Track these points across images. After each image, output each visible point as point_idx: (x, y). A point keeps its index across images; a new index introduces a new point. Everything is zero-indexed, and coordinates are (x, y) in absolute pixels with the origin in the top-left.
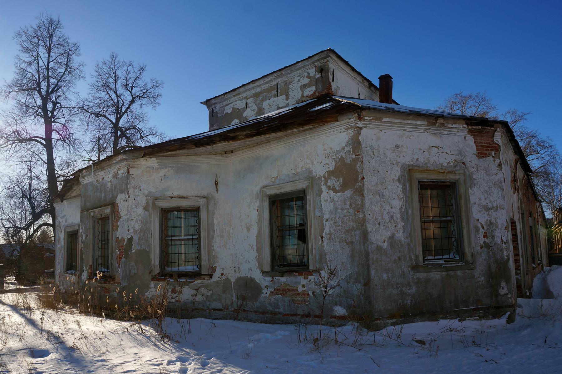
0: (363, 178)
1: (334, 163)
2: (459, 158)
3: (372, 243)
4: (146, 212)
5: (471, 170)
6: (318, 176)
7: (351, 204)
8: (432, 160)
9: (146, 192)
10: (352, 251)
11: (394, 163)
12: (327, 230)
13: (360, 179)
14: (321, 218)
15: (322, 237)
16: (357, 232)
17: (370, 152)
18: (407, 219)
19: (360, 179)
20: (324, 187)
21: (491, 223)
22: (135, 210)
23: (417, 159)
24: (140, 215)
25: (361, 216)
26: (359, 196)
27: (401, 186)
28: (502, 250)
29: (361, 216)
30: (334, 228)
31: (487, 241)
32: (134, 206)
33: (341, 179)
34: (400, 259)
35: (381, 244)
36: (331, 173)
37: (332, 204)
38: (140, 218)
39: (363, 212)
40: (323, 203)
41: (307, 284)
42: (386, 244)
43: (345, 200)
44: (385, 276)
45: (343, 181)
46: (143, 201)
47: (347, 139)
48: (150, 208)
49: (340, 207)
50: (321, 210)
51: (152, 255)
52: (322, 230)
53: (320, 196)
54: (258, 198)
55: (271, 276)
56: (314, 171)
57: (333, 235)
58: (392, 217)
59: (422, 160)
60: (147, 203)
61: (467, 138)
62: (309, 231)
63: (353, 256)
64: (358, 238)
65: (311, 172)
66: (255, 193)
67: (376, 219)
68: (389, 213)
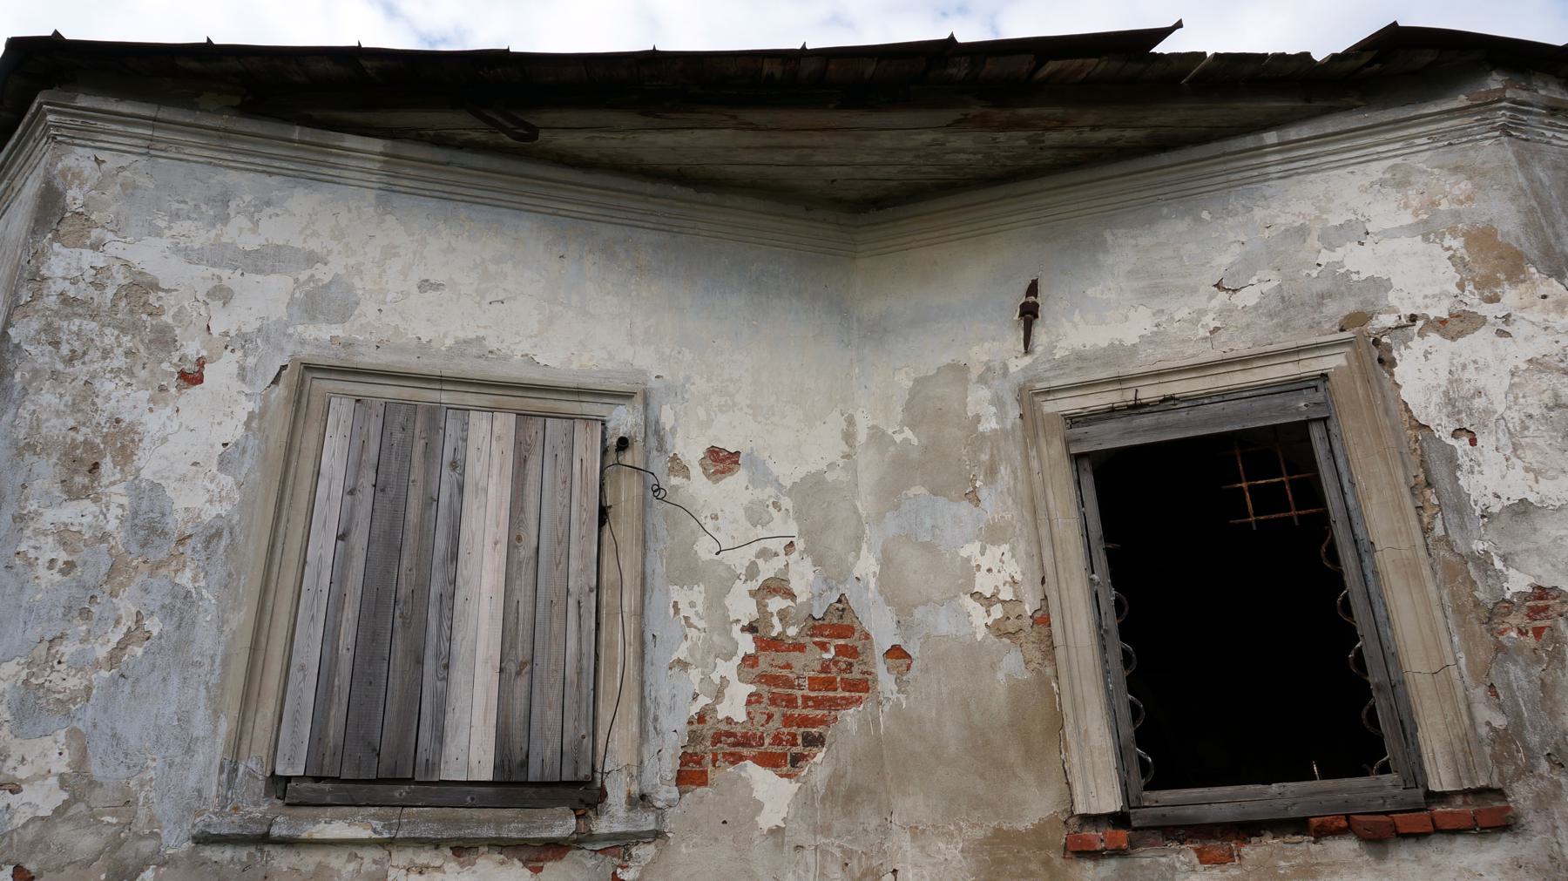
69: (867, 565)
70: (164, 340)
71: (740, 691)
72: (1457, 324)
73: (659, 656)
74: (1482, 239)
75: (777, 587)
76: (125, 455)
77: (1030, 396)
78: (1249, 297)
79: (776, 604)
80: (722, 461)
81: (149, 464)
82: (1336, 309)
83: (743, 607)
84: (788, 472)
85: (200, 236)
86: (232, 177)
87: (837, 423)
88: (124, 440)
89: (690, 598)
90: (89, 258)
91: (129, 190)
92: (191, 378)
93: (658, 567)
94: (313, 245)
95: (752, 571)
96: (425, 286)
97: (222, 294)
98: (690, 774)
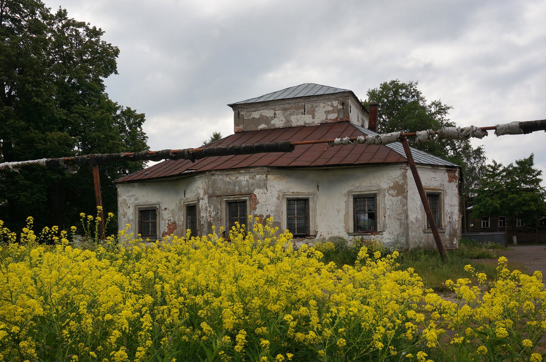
0: (407, 192)
1: (393, 183)
4: (278, 201)
6: (384, 188)
7: (401, 203)
9: (278, 190)
10: (400, 223)
12: (388, 213)
13: (406, 192)
14: (385, 208)
15: (385, 217)
16: (404, 215)
17: (410, 180)
19: (406, 192)
20: (387, 194)
21: (452, 213)
24: (274, 202)
25: (405, 208)
26: (405, 199)
29: (405, 208)
30: (392, 213)
32: (271, 197)
33: (396, 191)
36: (391, 188)
37: (391, 202)
38: (274, 204)
39: (407, 206)
40: (386, 201)
41: (376, 238)
43: (398, 201)
45: (397, 192)
46: (276, 194)
47: (400, 173)
48: (281, 198)
49: (395, 203)
50: (385, 204)
52: (385, 213)
53: (384, 198)
54: (346, 196)
55: (353, 236)
56: (381, 186)
57: (391, 216)
60: (279, 196)
62: (378, 213)
63: (401, 225)
64: (403, 217)
65: (379, 186)
66: (344, 193)
69: (177, 217)
70: (127, 205)
71: (167, 229)
72: (203, 199)
73: (161, 227)
74: (205, 190)
75: (170, 220)
76: (126, 215)
77: (184, 202)
78: (195, 194)
79: (170, 222)
80: (166, 209)
81: (128, 215)
82: (198, 196)
83: (167, 222)
84: (171, 209)
85: (127, 195)
86: (129, 189)
87: (175, 203)
88: (126, 213)
89: (163, 222)
90: (122, 198)
91: (123, 191)
92: (129, 208)
93: (161, 219)
94: (135, 194)
95: (168, 219)
96: (143, 196)
97: (130, 200)
98: (163, 236)
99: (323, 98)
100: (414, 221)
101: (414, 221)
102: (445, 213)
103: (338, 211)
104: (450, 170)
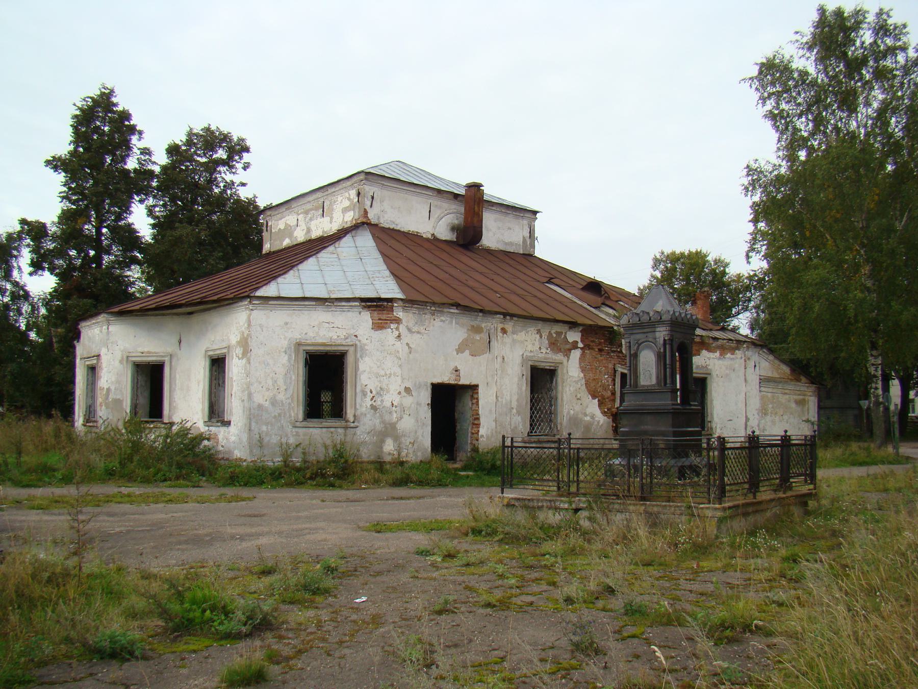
2: (352, 331)
3: (254, 402)
5: (364, 341)
8: (321, 334)
9: (122, 348)
11: (282, 337)
17: (259, 329)
18: (290, 383)
22: (113, 363)
23: (306, 334)
27: (286, 357)
28: (390, 413)
31: (374, 404)
34: (280, 415)
35: (261, 401)
42: (267, 403)
44: (264, 428)
46: (118, 355)
51: (124, 404)
58: (276, 381)
59: (311, 334)
61: (362, 313)
67: (260, 383)
68: (272, 378)
99: (340, 187)
100: (267, 404)
101: (267, 404)
102: (358, 390)
103: (199, 383)
104: (376, 306)
